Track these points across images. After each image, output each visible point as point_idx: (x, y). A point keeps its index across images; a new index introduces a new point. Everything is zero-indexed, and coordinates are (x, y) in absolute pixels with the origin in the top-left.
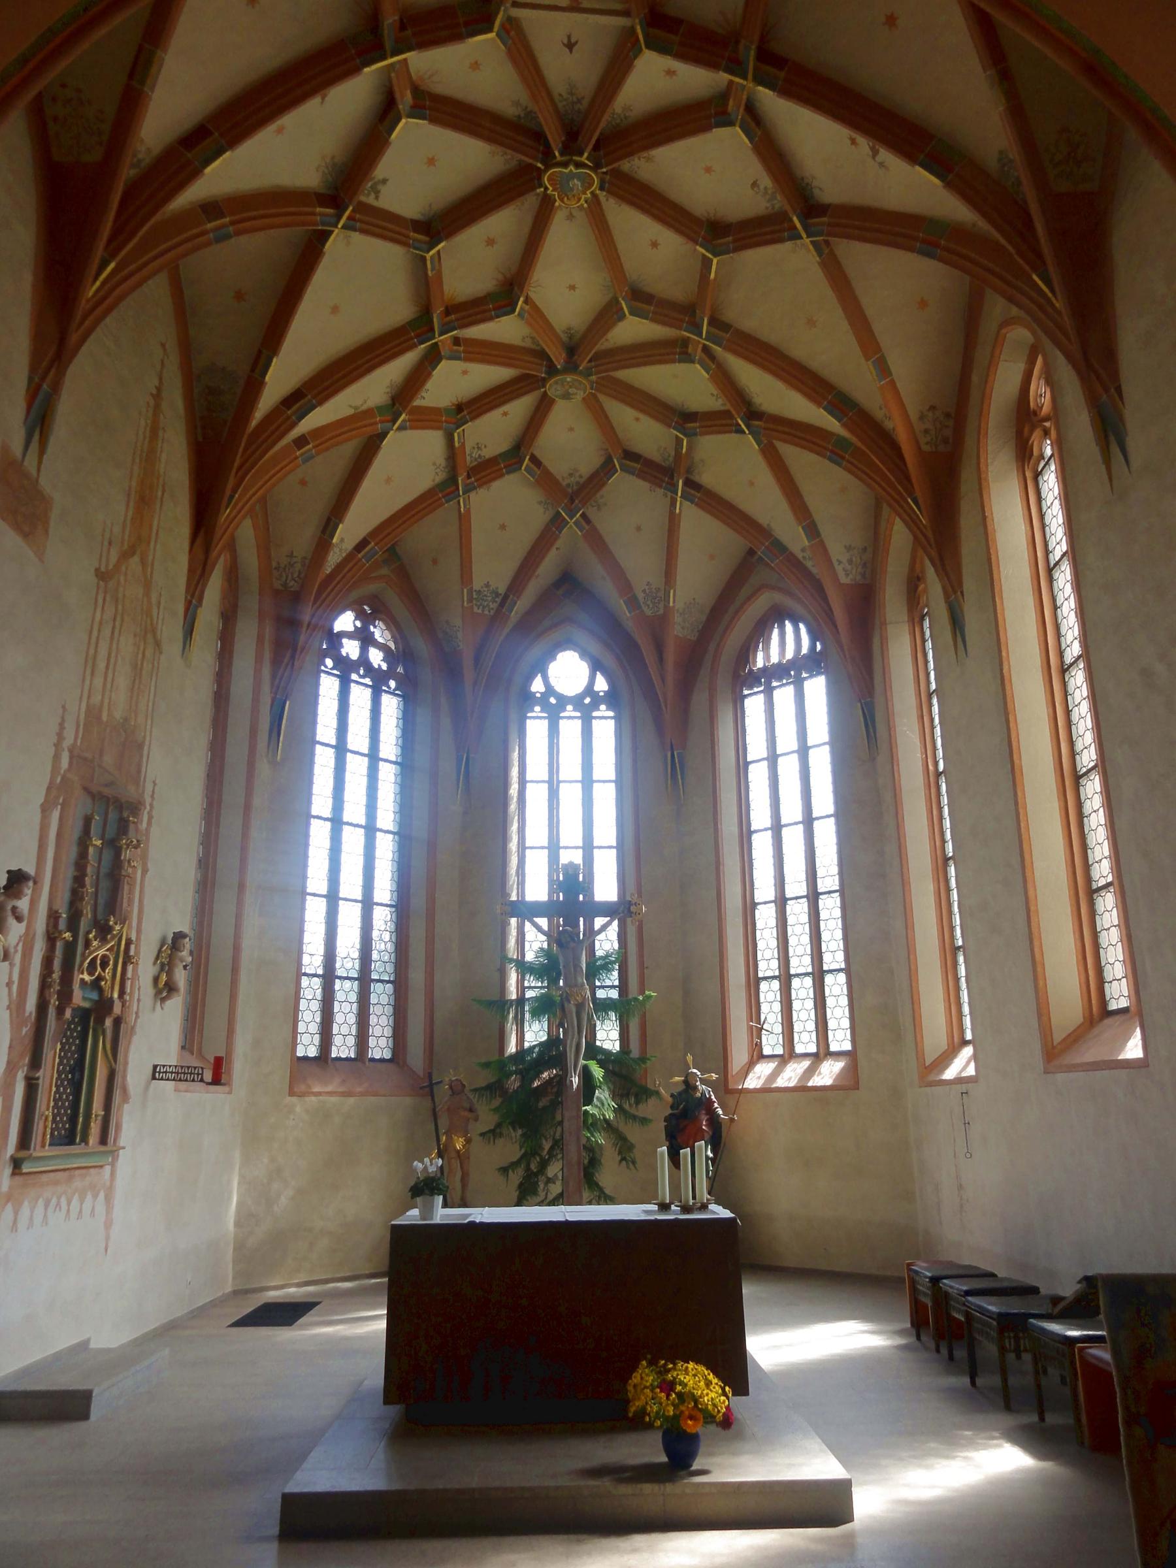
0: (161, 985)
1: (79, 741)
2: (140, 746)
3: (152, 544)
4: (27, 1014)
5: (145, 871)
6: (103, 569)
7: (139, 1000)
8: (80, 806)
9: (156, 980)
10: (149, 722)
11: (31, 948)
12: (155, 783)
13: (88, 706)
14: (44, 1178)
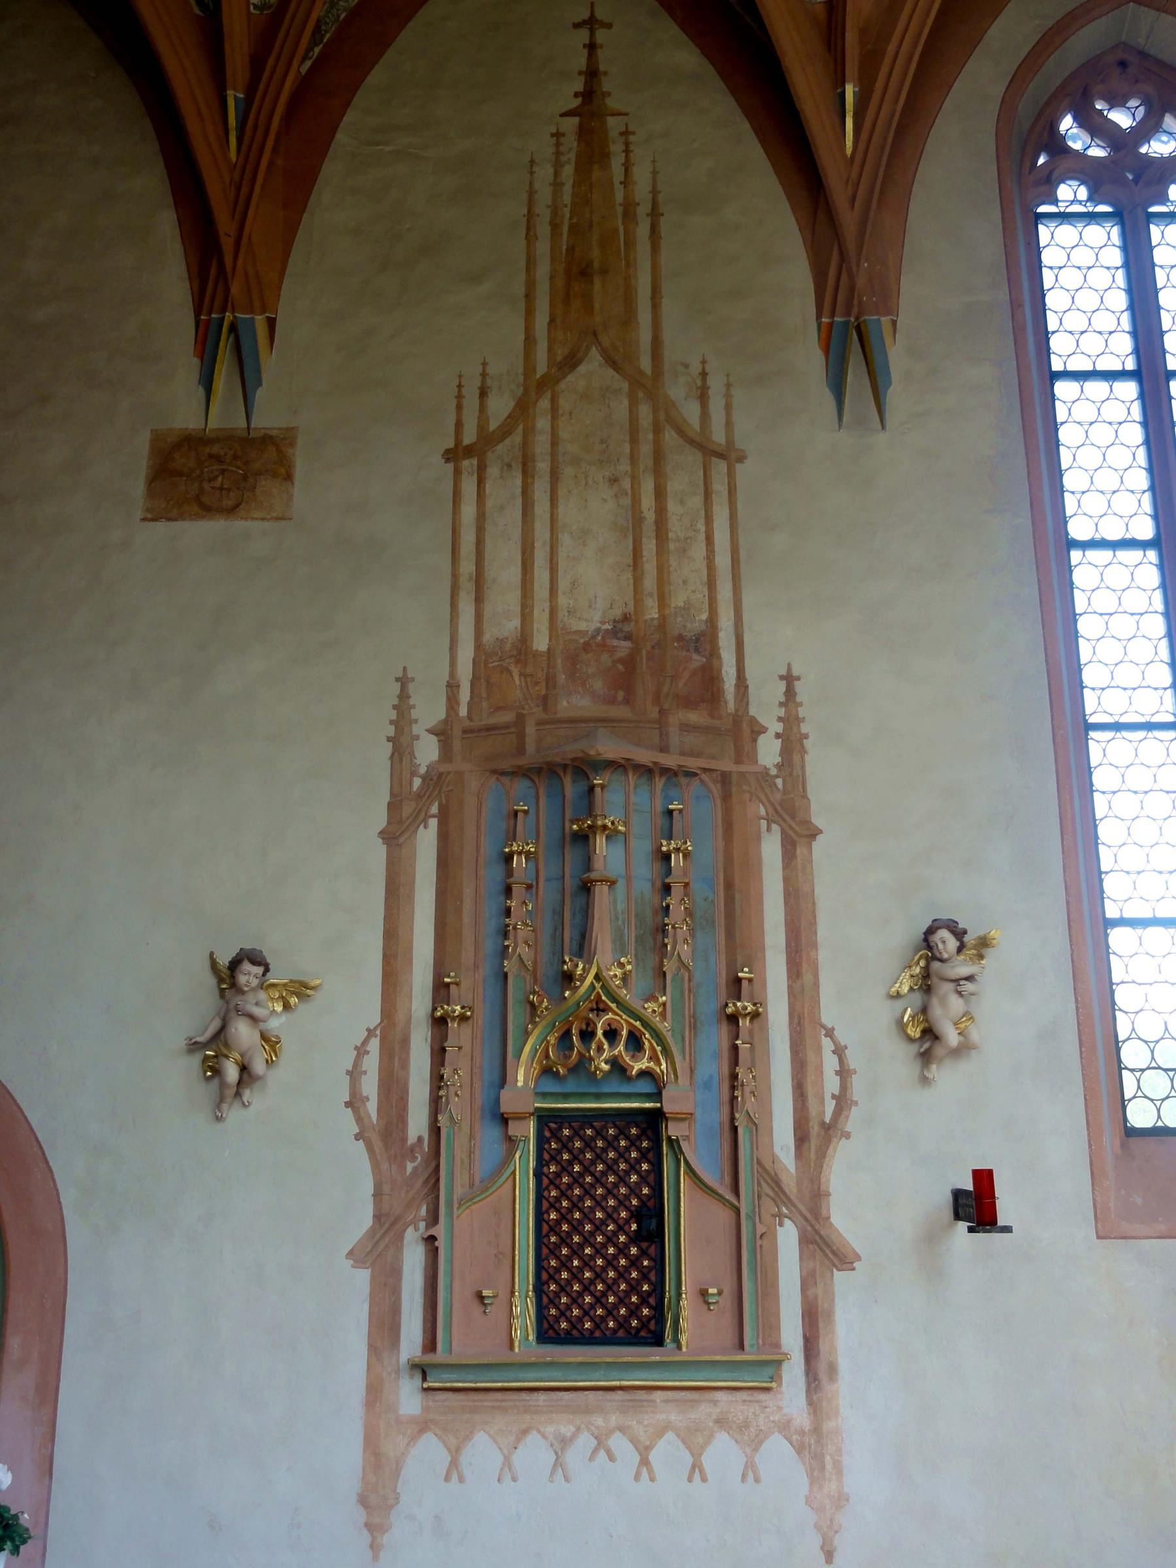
0: (914, 1032)
1: (463, 711)
2: (706, 640)
3: (644, 316)
4: (412, 1137)
5: (799, 834)
6: (469, 437)
7: (844, 1073)
8: (484, 802)
9: (901, 1026)
10: (725, 592)
11: (405, 1042)
12: (789, 679)
13: (478, 647)
14: (542, 1397)
